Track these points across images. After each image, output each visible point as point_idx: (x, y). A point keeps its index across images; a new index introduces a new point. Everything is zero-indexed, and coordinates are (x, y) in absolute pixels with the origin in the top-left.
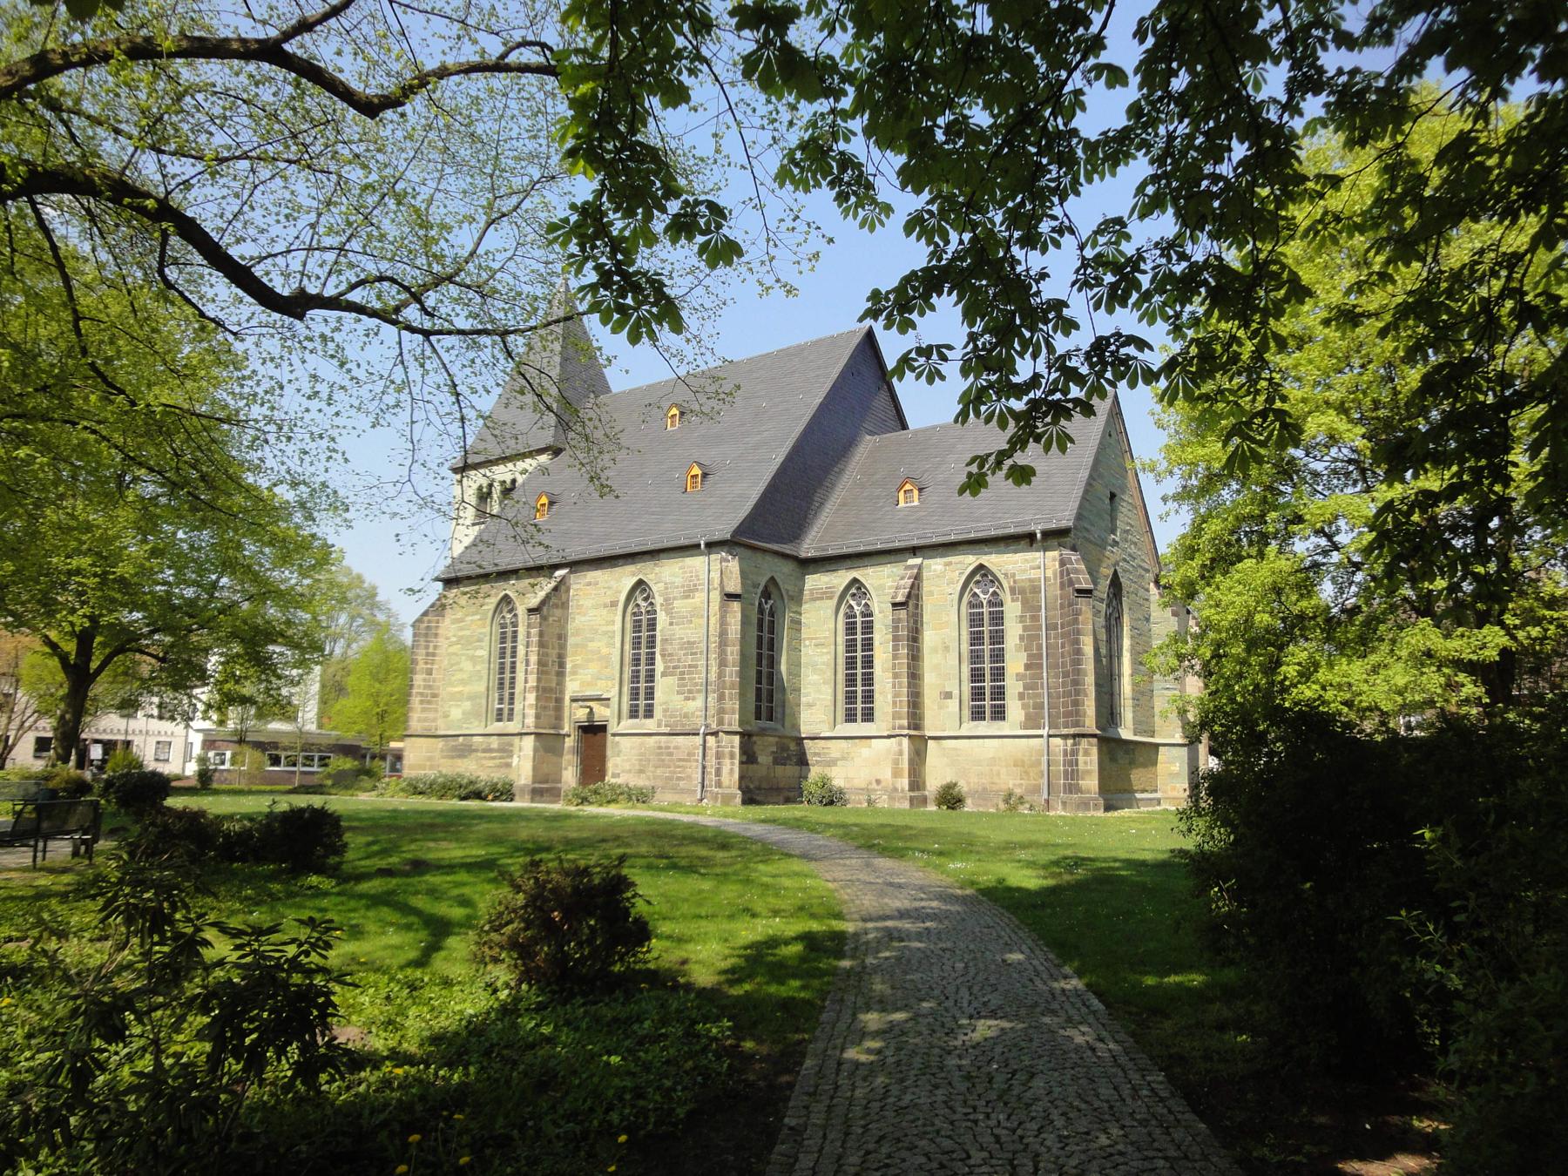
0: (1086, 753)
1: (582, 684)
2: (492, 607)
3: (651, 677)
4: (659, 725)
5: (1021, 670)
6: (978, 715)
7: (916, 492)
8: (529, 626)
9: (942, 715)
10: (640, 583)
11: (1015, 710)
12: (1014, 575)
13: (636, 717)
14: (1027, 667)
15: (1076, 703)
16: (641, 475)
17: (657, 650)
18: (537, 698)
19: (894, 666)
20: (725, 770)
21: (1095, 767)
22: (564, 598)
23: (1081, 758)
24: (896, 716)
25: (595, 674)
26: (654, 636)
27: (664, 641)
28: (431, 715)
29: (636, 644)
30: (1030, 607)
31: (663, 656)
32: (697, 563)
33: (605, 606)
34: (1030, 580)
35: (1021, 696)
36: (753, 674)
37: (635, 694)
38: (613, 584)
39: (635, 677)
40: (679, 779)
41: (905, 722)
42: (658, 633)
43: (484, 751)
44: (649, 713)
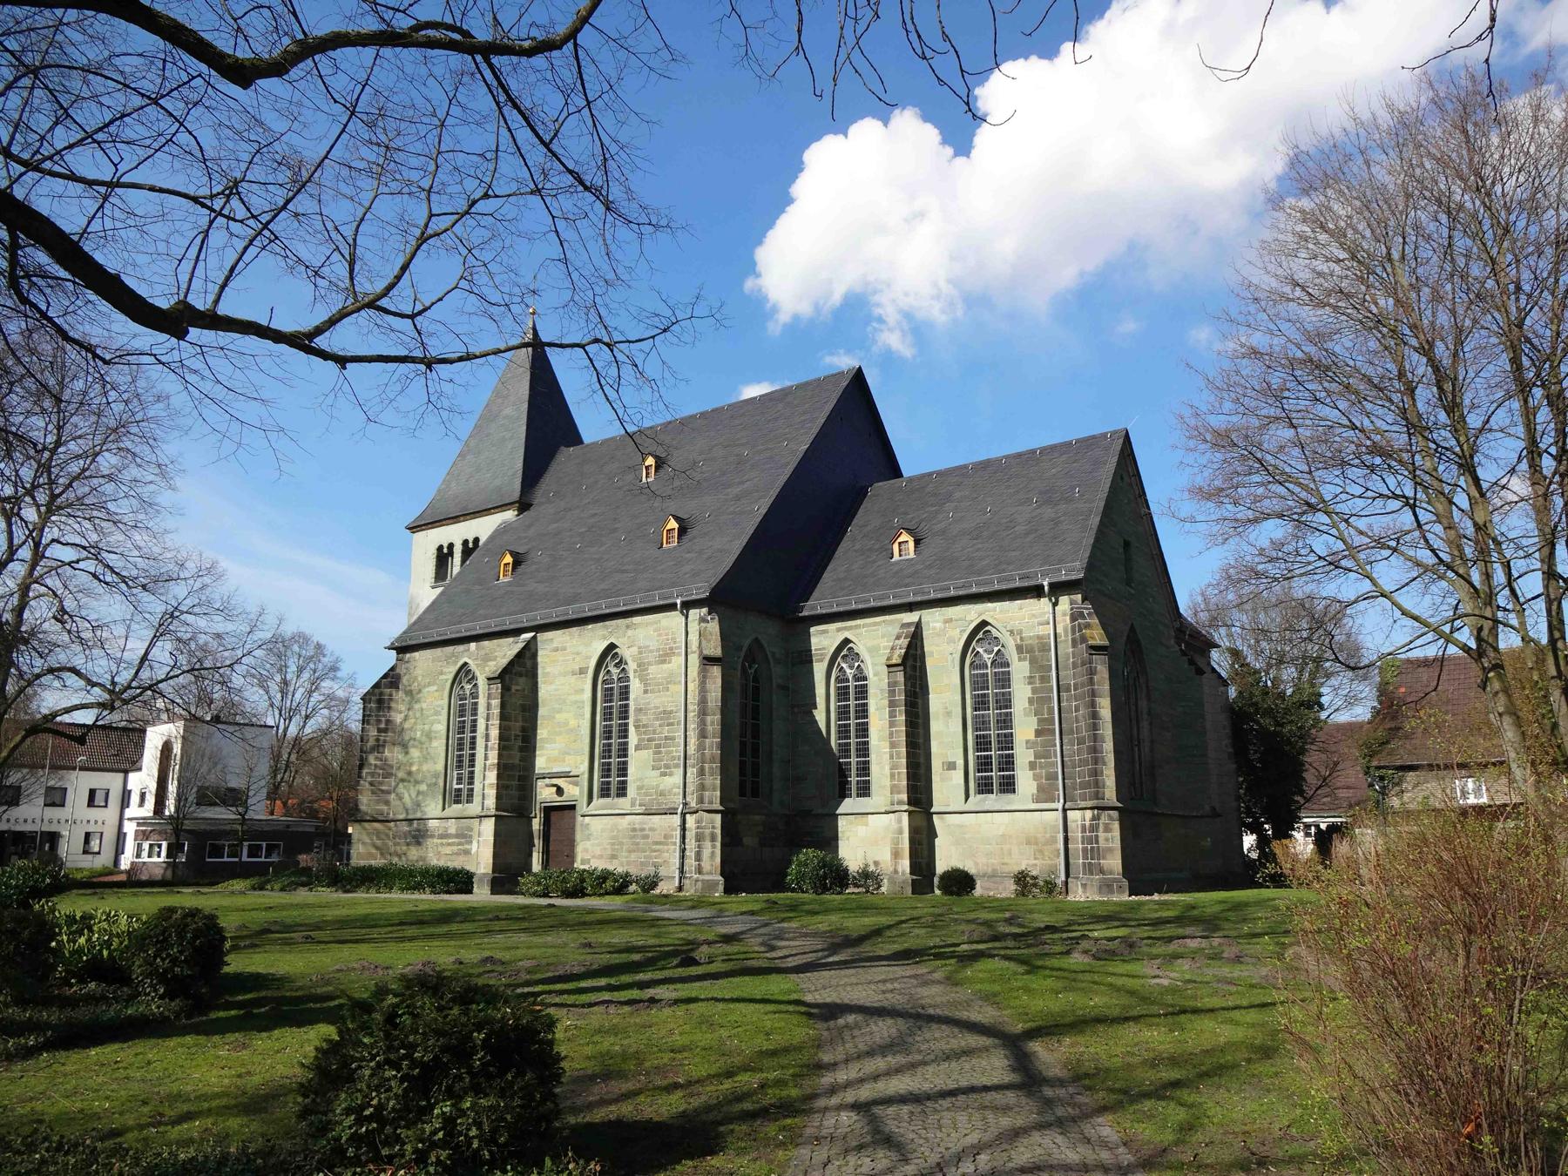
0: (1107, 829)
1: (549, 760)
2: (451, 677)
3: (623, 751)
4: (633, 804)
5: (1032, 736)
6: (985, 787)
7: (911, 544)
8: (489, 697)
9: (947, 788)
10: (612, 646)
11: (1026, 781)
12: (1020, 632)
13: (608, 796)
14: (1038, 733)
15: (1095, 773)
16: (615, 530)
17: (631, 721)
18: (499, 777)
19: (891, 734)
20: (706, 853)
21: (1117, 844)
22: (529, 664)
23: (1102, 835)
24: (894, 790)
25: (562, 749)
26: (627, 706)
27: (639, 710)
29: (608, 715)
30: (1039, 668)
31: (637, 727)
32: (674, 620)
33: (574, 674)
34: (1039, 637)
35: (1032, 766)
36: (737, 745)
37: (606, 771)
38: (581, 648)
39: (607, 752)
41: (904, 797)
42: (631, 703)
43: (441, 837)
44: (622, 791)
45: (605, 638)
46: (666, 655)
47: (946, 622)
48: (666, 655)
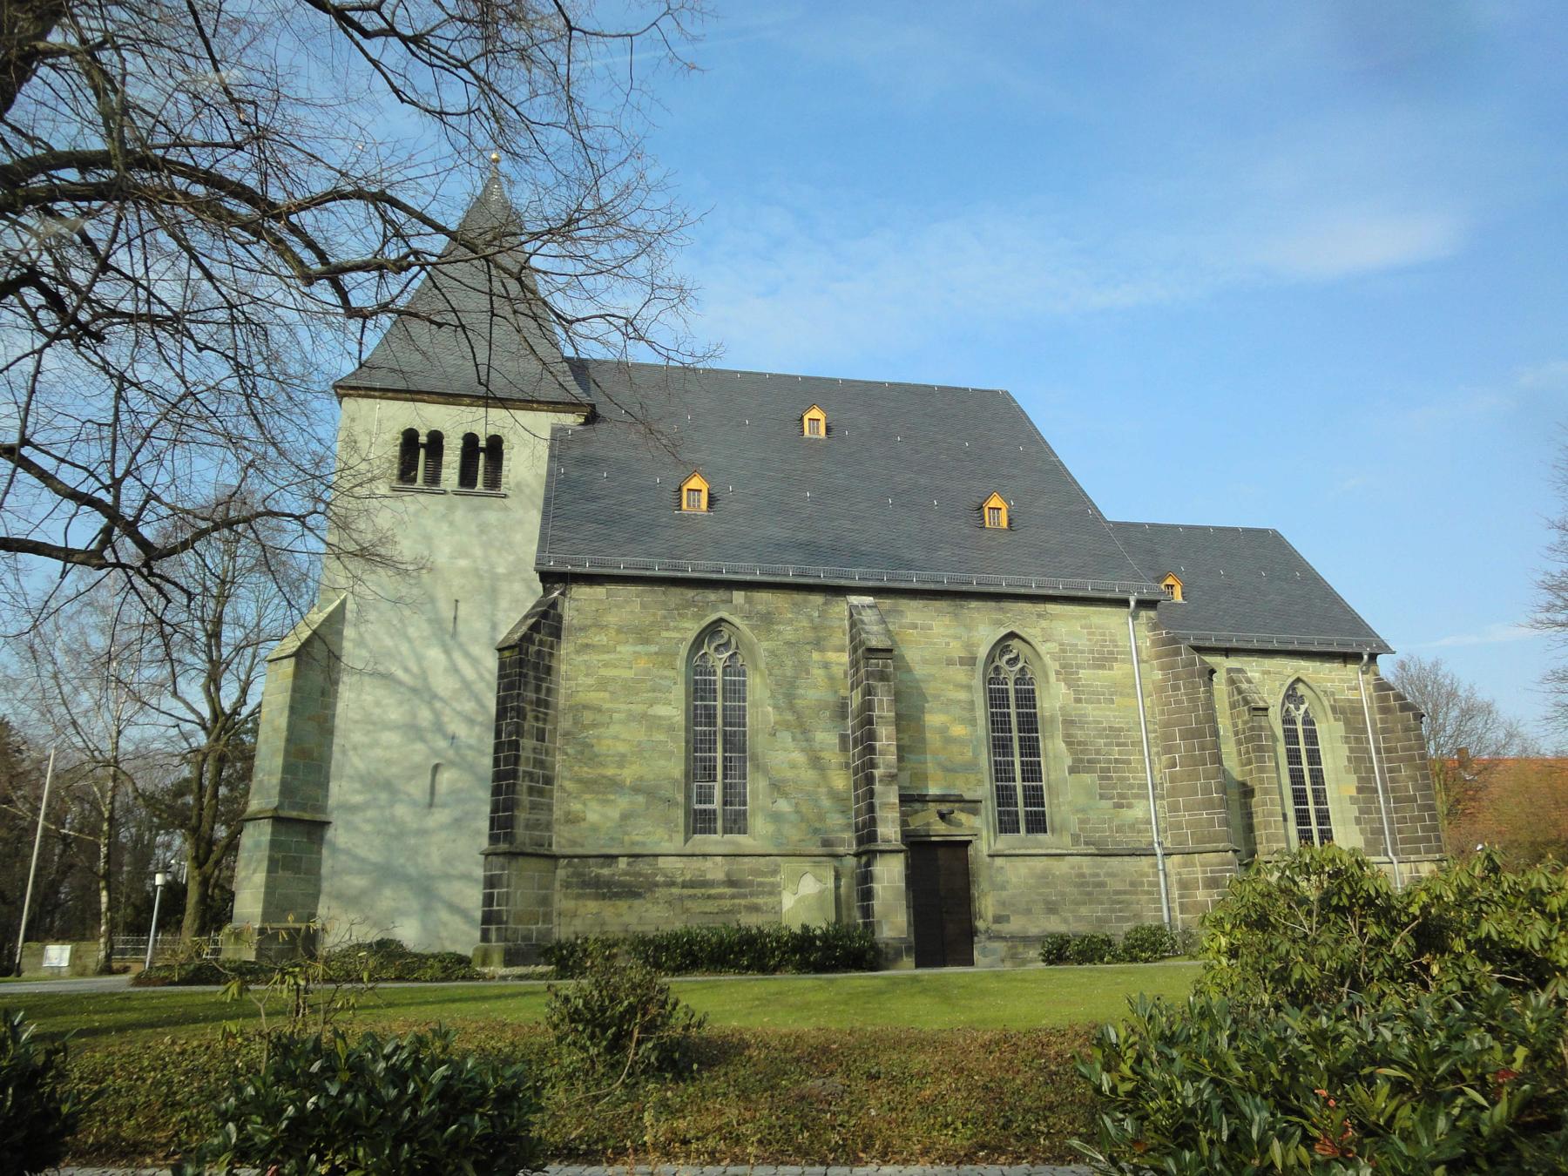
4: (1076, 839)
14: (1360, 790)
27: (1069, 723)
28: (543, 817)
30: (1354, 730)
40: (1119, 919)
45: (1000, 623)
46: (1106, 659)
47: (1264, 673)
48: (1106, 659)
